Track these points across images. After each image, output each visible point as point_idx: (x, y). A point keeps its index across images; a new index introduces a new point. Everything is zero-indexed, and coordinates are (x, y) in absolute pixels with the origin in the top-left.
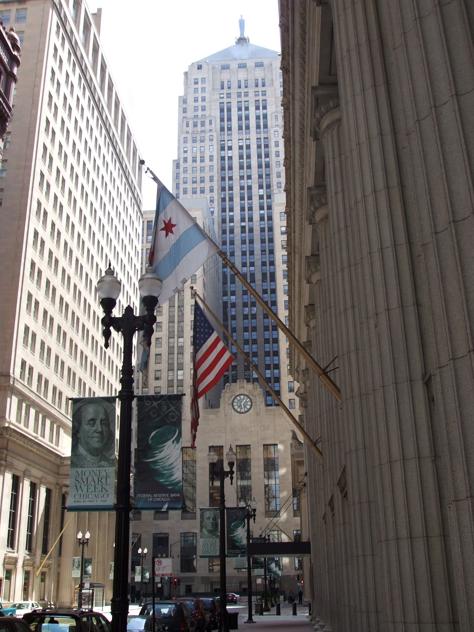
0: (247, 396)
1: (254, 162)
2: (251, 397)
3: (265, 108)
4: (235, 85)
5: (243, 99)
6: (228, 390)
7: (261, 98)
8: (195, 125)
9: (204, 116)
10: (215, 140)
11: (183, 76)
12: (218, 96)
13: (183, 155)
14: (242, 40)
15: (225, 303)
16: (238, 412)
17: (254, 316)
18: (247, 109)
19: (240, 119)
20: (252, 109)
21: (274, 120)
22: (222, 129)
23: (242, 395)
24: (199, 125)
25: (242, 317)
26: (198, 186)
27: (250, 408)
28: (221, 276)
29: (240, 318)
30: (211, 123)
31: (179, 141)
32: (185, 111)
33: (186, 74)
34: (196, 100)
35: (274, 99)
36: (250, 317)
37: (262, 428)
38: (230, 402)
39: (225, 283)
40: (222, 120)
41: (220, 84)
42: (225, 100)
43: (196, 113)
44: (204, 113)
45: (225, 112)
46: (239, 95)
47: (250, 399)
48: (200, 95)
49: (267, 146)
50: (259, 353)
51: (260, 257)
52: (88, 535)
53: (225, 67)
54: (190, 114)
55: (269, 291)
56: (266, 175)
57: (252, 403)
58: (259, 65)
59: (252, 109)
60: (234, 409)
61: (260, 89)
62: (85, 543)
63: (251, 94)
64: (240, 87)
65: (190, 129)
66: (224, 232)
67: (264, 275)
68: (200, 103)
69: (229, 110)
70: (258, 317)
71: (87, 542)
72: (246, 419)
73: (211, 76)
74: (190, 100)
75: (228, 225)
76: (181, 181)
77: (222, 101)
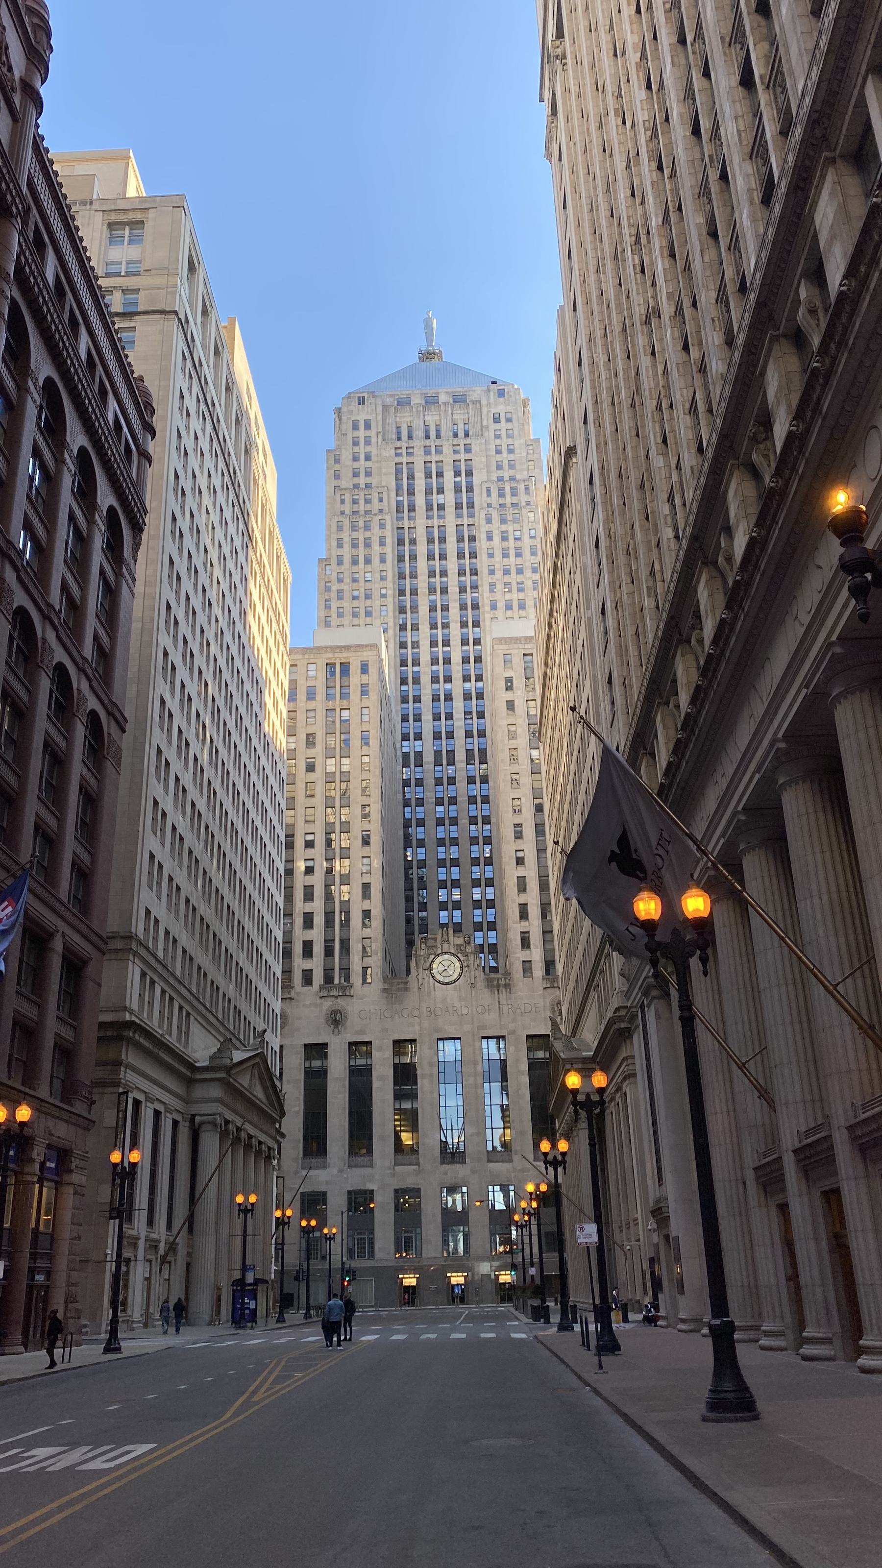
1: (452, 564)
2: (462, 958)
3: (469, 473)
4: (419, 433)
5: (434, 458)
6: (423, 946)
7: (463, 456)
8: (355, 502)
9: (368, 486)
10: (388, 527)
11: (333, 416)
12: (393, 452)
13: (335, 552)
18: (440, 475)
20: (449, 475)
21: (485, 494)
24: (362, 502)
26: (361, 604)
30: (381, 500)
31: (328, 528)
32: (337, 477)
33: (339, 411)
34: (356, 459)
35: (484, 459)
36: (447, 822)
37: (480, 1010)
38: (427, 964)
41: (394, 430)
42: (404, 460)
43: (356, 480)
44: (368, 480)
46: (427, 452)
47: (459, 960)
48: (362, 449)
49: (472, 539)
51: (462, 723)
52: (253, 1199)
54: (346, 482)
55: (478, 779)
56: (472, 588)
57: (462, 967)
58: (459, 400)
61: (462, 441)
62: (249, 1211)
63: (447, 450)
64: (427, 437)
65: (347, 508)
66: (404, 682)
68: (362, 464)
69: (411, 477)
71: (252, 1210)
73: (380, 418)
74: (346, 456)
75: (410, 669)
76: (334, 595)
77: (398, 460)
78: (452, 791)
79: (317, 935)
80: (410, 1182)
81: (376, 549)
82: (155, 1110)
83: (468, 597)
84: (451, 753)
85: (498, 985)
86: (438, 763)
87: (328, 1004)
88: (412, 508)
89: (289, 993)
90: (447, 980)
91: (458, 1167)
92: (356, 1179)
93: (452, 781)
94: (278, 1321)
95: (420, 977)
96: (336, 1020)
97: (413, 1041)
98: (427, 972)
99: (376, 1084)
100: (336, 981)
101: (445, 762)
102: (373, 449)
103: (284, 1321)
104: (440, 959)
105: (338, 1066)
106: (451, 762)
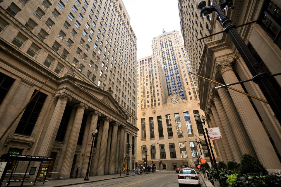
3: (171, 41)
14: (164, 32)
15: (167, 85)
17: (175, 87)
18: (167, 43)
19: (165, 45)
20: (168, 42)
22: (162, 49)
25: (172, 87)
29: (172, 88)
38: (170, 101)
39: (167, 80)
40: (161, 47)
45: (162, 45)
53: (161, 37)
54: (154, 47)
59: (168, 42)
67: (177, 77)
68: (156, 45)
69: (163, 44)
72: (176, 105)
78: (176, 88)
79: (150, 99)
80: (172, 142)
81: (158, 53)
82: (133, 136)
83: (173, 56)
84: (174, 77)
85: (185, 102)
86: (172, 79)
87: (153, 110)
88: (163, 48)
91: (182, 138)
92: (161, 142)
93: (174, 81)
94: (85, 180)
96: (154, 112)
97: (169, 115)
99: (163, 123)
102: (157, 43)
103: (88, 180)
104: (173, 99)
105: (155, 121)
106: (174, 79)
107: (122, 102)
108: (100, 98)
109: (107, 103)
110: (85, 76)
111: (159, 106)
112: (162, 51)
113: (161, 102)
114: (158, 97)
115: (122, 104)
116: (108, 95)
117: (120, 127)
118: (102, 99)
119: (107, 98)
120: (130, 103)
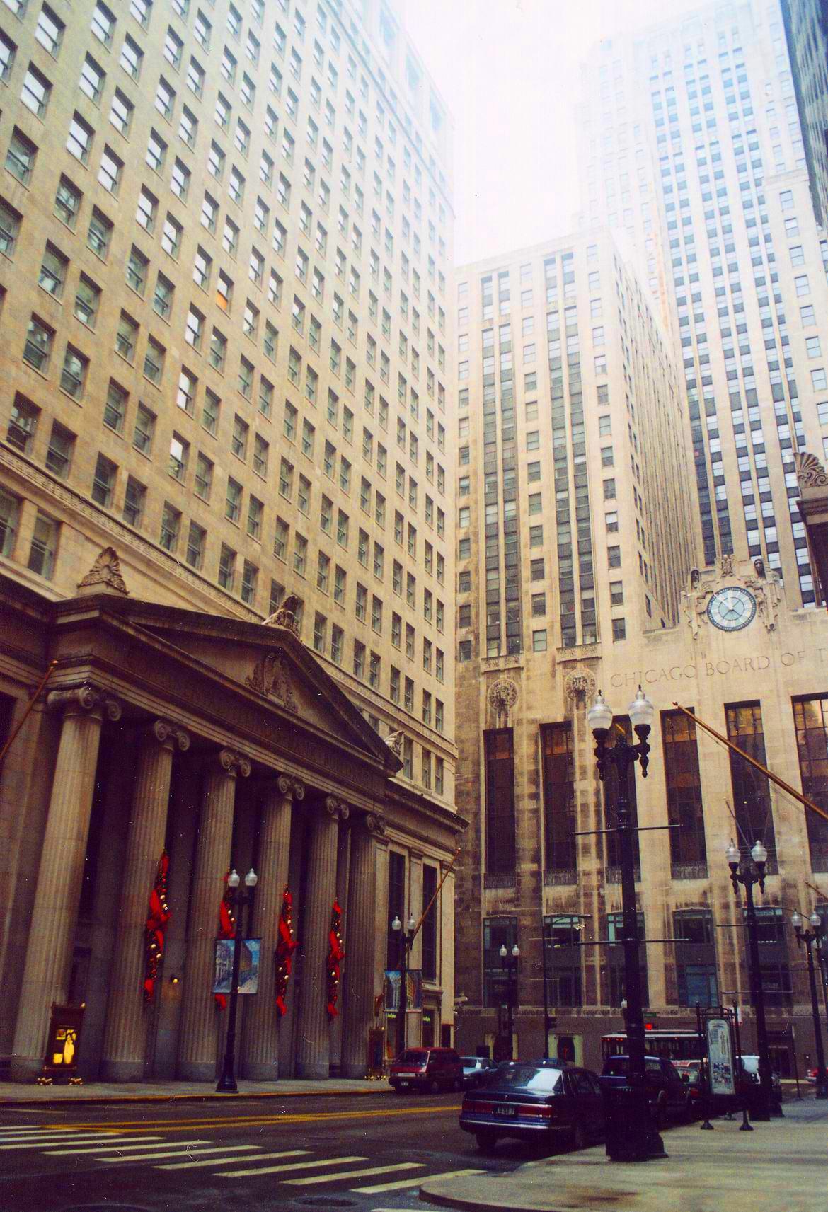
0: (741, 589)
16: (722, 628)
23: (729, 589)
25: (736, 478)
27: (752, 616)
28: (686, 405)
29: (732, 478)
47: (750, 595)
50: (780, 544)
60: (713, 622)
70: (771, 472)
84: (751, 393)
86: (735, 407)
89: (516, 662)
90: (733, 624)
95: (694, 624)
98: (705, 617)
100: (579, 641)
101: (744, 404)
106: (753, 404)
107: (356, 655)
108: (240, 672)
109: (280, 697)
110: (151, 545)
111: (619, 643)
112: (667, 181)
113: (630, 611)
114: (616, 574)
115: (357, 666)
116: (276, 648)
117: (358, 830)
118: (252, 676)
119: (277, 663)
120: (410, 594)
